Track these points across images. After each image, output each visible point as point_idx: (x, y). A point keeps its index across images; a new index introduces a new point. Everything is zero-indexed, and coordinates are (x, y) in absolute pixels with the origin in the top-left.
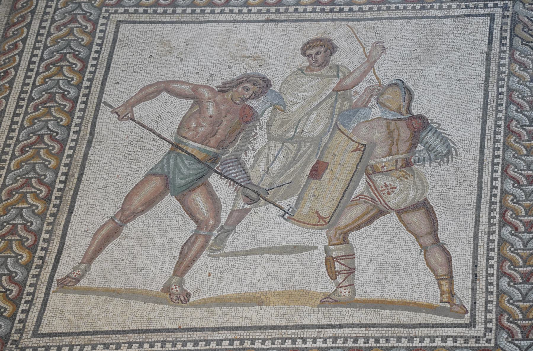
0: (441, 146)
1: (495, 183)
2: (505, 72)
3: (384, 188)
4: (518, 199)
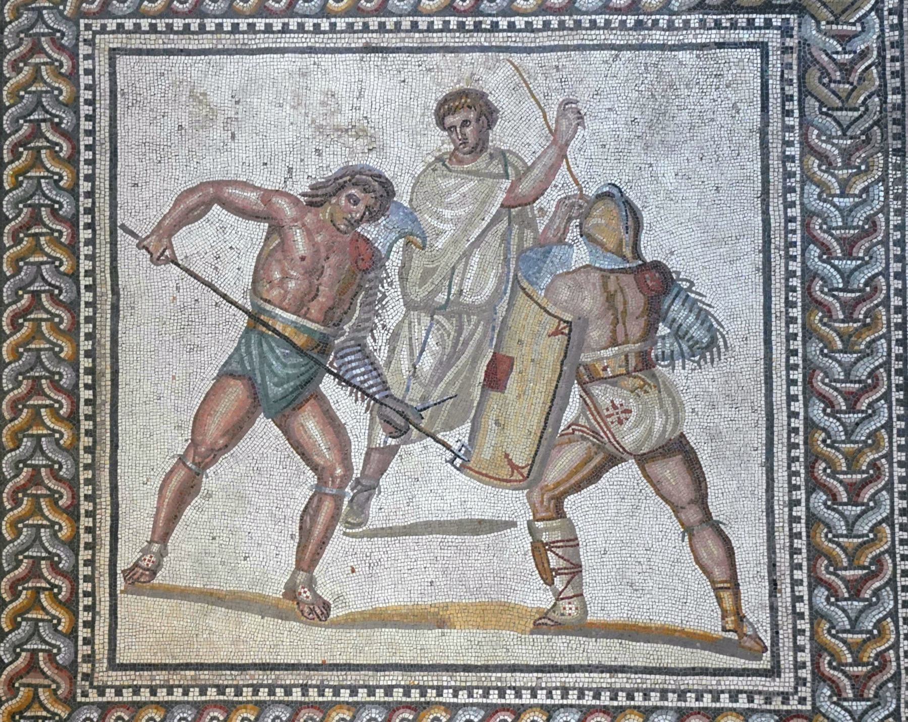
0: (699, 329)
2: (795, 174)
3: (611, 411)
4: (833, 438)
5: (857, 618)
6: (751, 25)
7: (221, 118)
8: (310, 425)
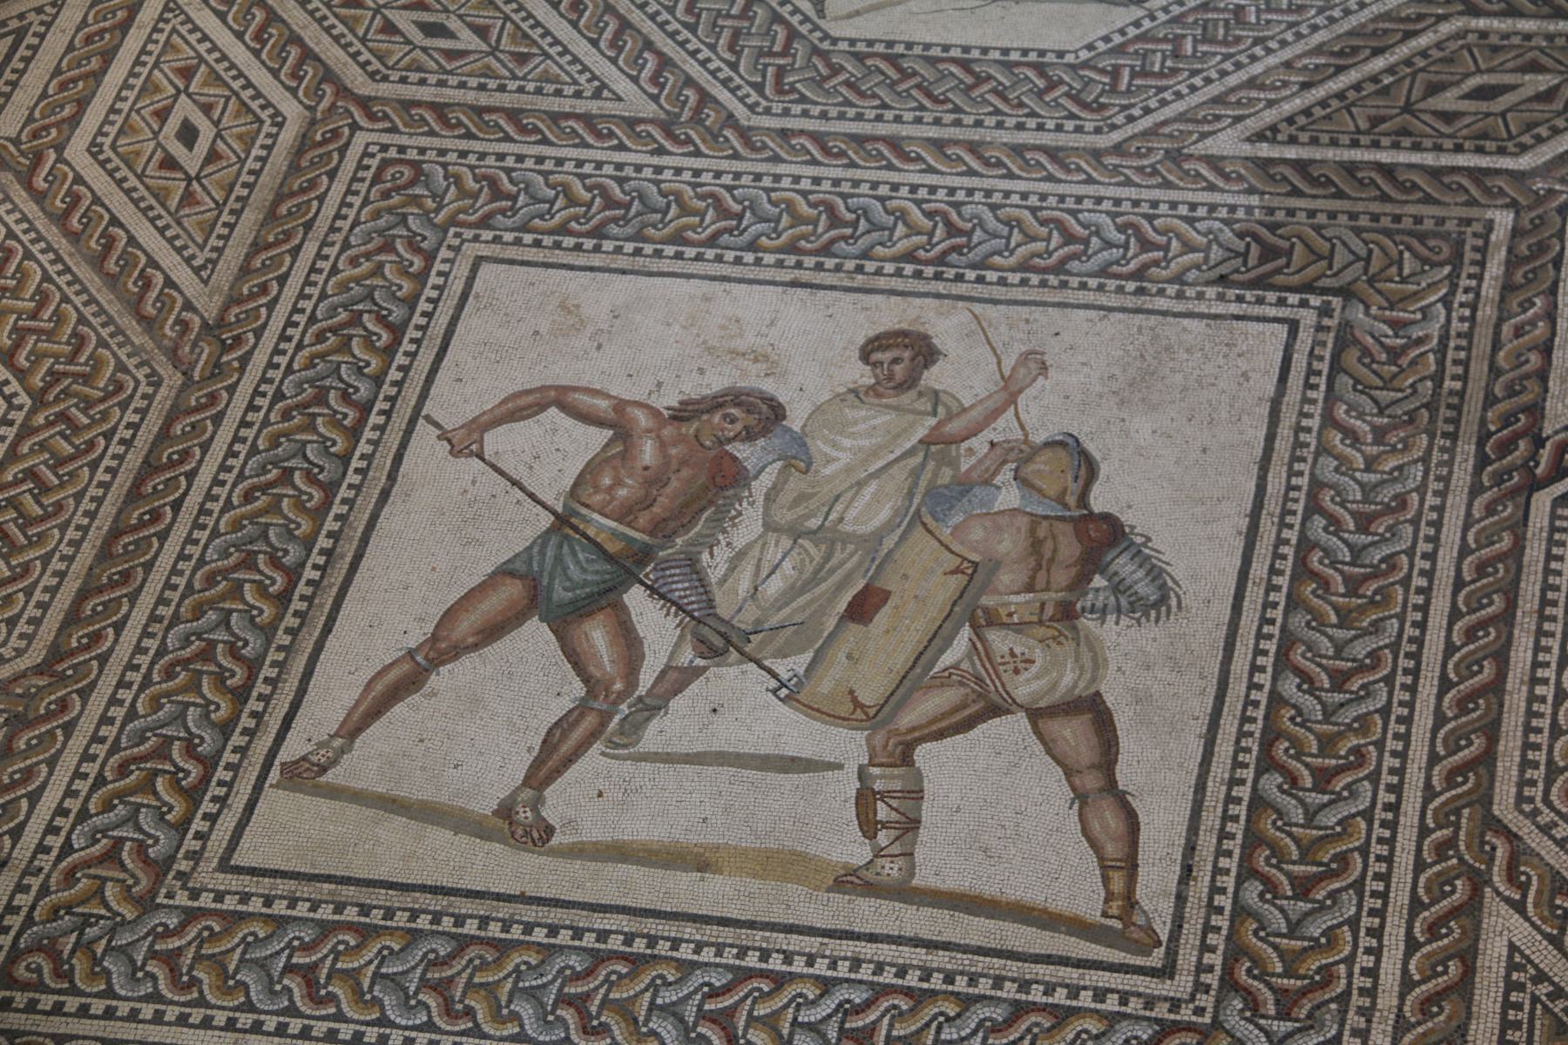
1: (1258, 678)
5: (1299, 922)
6: (1281, 302)
7: (590, 329)
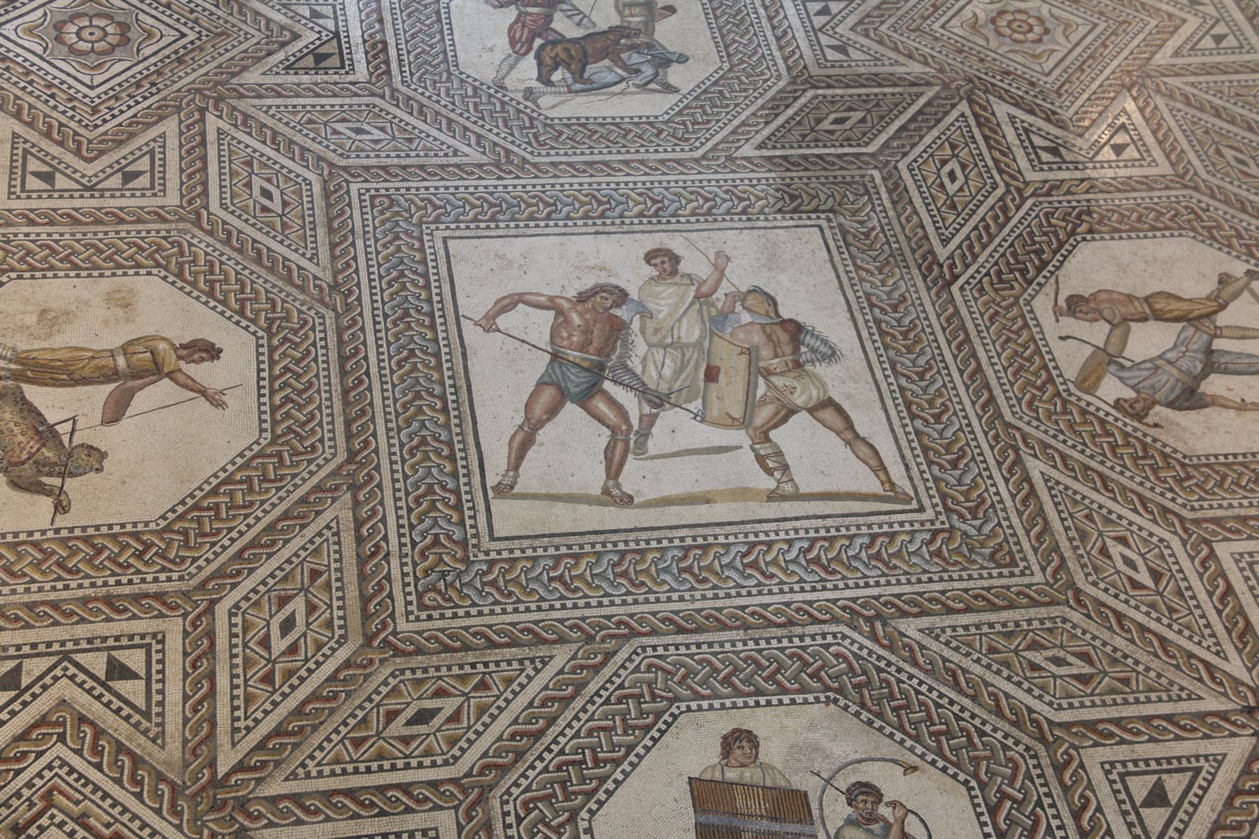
8: (601, 406)
